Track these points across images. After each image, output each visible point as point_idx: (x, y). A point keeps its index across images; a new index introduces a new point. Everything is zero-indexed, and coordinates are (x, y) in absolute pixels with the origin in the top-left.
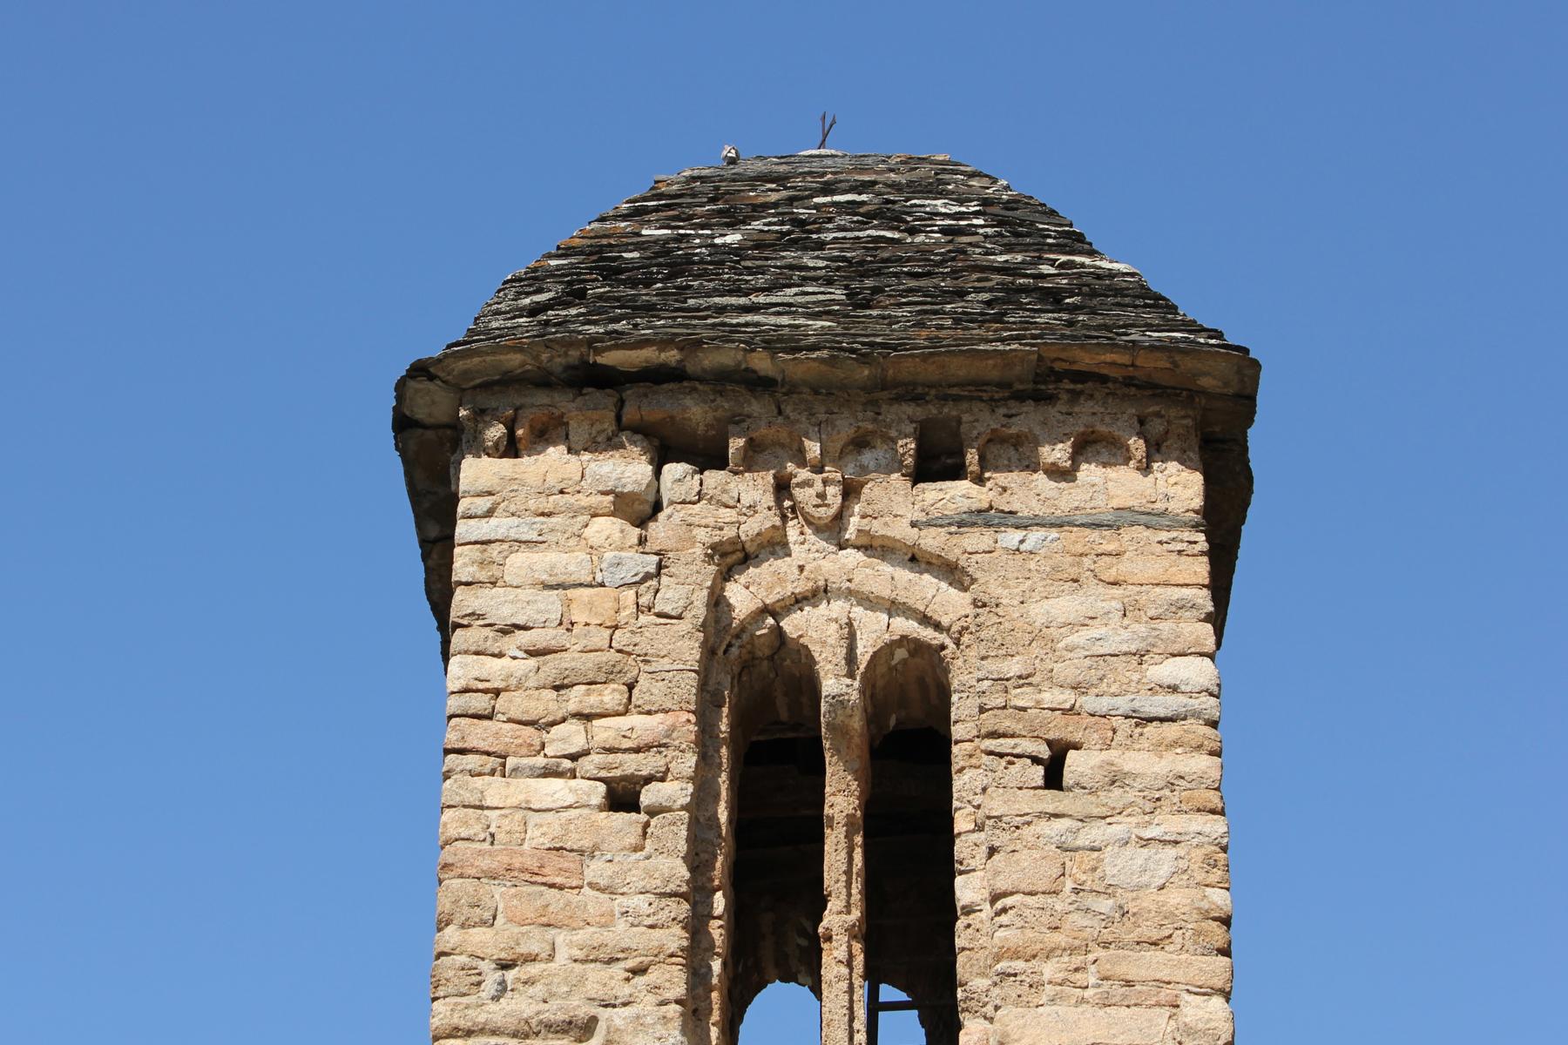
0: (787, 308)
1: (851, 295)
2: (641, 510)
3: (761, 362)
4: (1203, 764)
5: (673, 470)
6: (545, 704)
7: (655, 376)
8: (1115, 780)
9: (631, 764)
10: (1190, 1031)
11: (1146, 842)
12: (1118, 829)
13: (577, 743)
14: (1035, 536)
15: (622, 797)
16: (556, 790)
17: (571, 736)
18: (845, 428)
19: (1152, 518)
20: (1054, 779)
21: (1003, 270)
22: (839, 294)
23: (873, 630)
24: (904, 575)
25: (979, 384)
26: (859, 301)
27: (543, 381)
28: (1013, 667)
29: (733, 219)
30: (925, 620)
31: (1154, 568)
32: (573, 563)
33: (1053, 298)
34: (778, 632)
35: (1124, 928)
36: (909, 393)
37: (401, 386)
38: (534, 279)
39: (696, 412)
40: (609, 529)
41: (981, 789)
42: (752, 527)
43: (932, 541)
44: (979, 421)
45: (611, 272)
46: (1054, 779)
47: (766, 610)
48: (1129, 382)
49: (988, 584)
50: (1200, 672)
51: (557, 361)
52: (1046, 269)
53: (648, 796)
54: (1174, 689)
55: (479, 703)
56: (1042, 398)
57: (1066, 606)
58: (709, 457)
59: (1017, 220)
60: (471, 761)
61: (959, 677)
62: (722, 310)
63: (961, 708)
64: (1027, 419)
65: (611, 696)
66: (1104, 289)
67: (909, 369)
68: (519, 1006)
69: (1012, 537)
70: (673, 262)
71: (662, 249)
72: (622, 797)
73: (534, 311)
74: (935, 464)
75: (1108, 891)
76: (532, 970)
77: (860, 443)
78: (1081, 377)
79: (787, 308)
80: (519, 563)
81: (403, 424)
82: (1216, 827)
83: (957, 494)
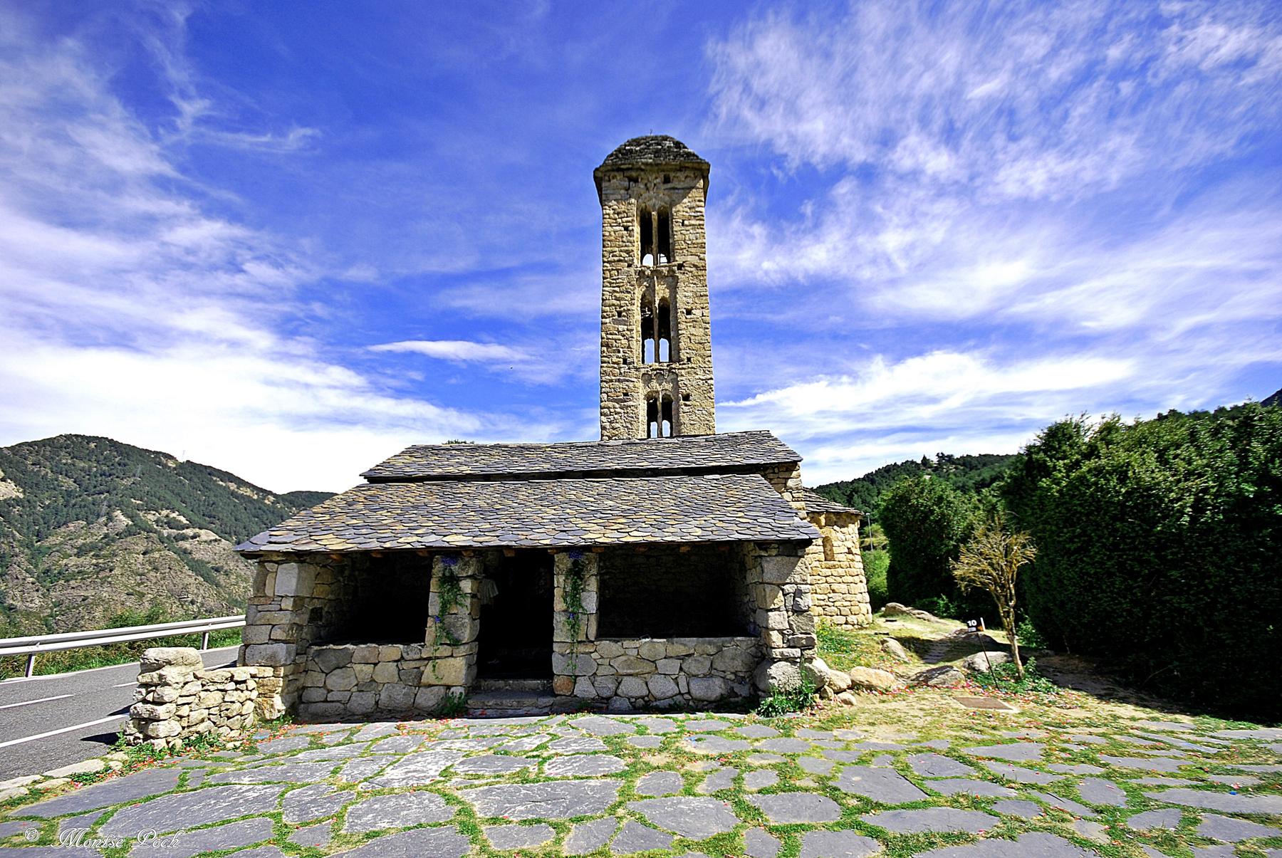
7: (628, 169)
29: (638, 145)
39: (634, 174)
58: (636, 181)
59: (678, 145)
66: (689, 154)
70: (631, 151)
72: (626, 229)
74: (667, 180)
83: (669, 185)
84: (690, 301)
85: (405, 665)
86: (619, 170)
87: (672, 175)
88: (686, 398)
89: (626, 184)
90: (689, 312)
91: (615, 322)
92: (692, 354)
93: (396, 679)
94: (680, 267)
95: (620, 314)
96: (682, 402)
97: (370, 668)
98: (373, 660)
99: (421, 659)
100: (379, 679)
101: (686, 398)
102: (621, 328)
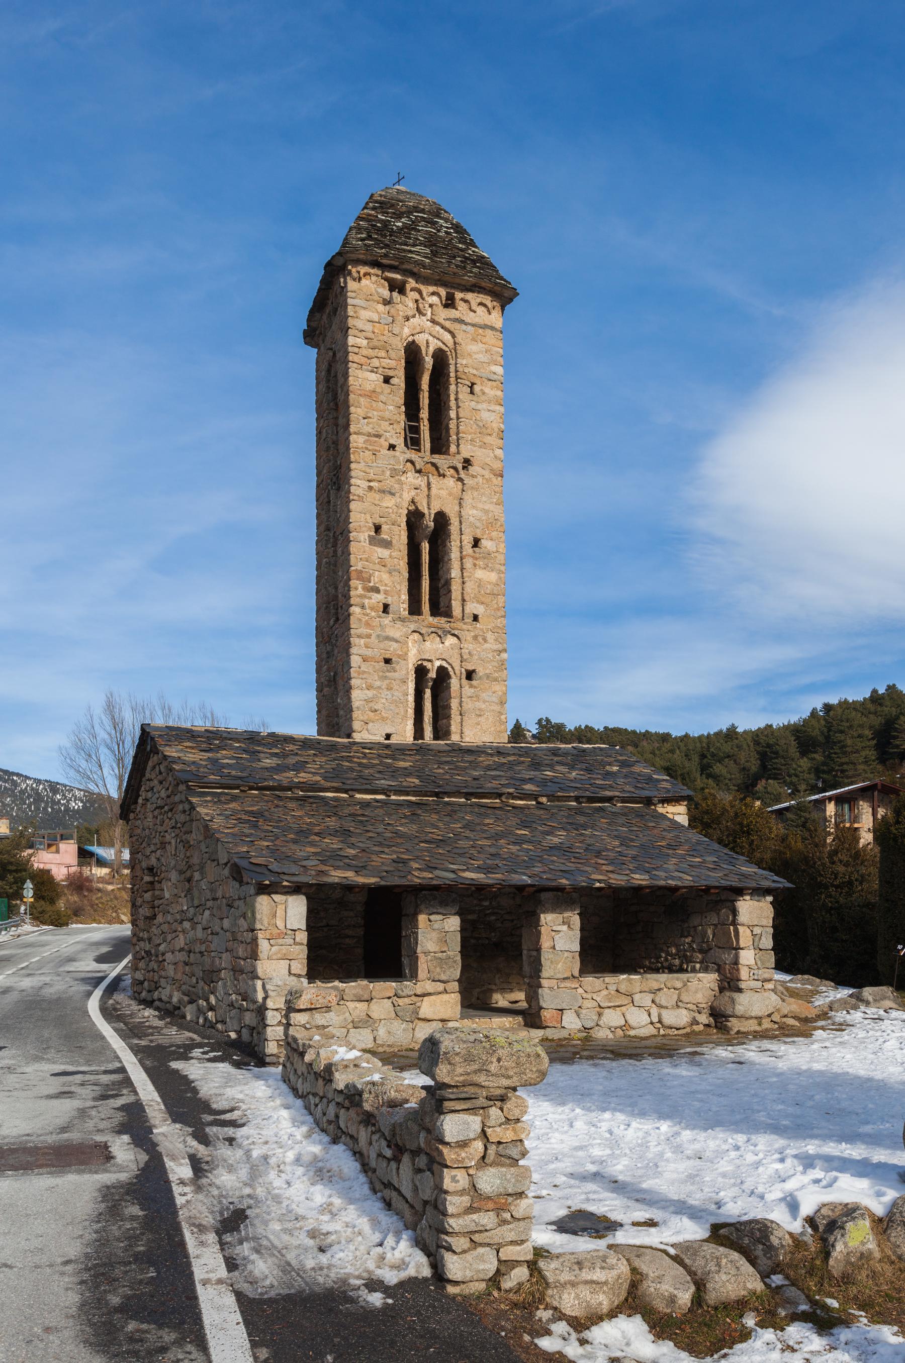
0: (418, 253)
1: (431, 251)
2: (387, 302)
3: (415, 270)
4: (499, 393)
5: (395, 294)
6: (370, 353)
8: (484, 393)
9: (391, 373)
10: (496, 457)
11: (489, 410)
12: (484, 406)
13: (377, 365)
14: (469, 328)
15: (387, 380)
16: (373, 376)
17: (376, 363)
18: (432, 289)
19: (492, 328)
20: (472, 393)
21: (462, 250)
22: (428, 251)
23: (434, 344)
24: (442, 331)
25: (459, 285)
26: (434, 254)
27: (365, 263)
28: (464, 362)
30: (444, 343)
31: (493, 341)
32: (375, 317)
33: (474, 262)
34: (414, 341)
35: (483, 429)
36: (444, 284)
37: (333, 257)
38: (359, 229)
40: (381, 307)
41: (456, 391)
42: (410, 313)
43: (448, 324)
44: (459, 295)
45: (379, 230)
46: (472, 393)
47: (413, 335)
48: (490, 291)
49: (459, 339)
50: (499, 370)
51: (370, 258)
52: (470, 252)
53: (392, 381)
54: (495, 373)
55: (356, 350)
56: (473, 292)
57: (473, 348)
58: (402, 291)
60: (355, 365)
61: (452, 362)
62: (405, 250)
63: (452, 369)
64: (470, 296)
65: (382, 354)
67: (447, 278)
68: (368, 429)
69: (464, 327)
71: (386, 224)
73: (362, 240)
75: (481, 421)
76: (370, 420)
77: (433, 294)
78: (480, 287)
79: (418, 253)
80: (365, 314)
81: (329, 265)
82: (502, 409)
83: (452, 313)
84: (478, 524)
85: (401, 1002)
86: (375, 264)
87: (459, 295)
88: (470, 675)
89: (386, 293)
90: (476, 543)
91: (373, 541)
92: (480, 610)
93: (394, 1015)
94: (467, 463)
95: (378, 528)
96: (464, 681)
97: (362, 1006)
98: (366, 997)
99: (416, 995)
100: (375, 1015)
101: (470, 675)
102: (384, 553)
